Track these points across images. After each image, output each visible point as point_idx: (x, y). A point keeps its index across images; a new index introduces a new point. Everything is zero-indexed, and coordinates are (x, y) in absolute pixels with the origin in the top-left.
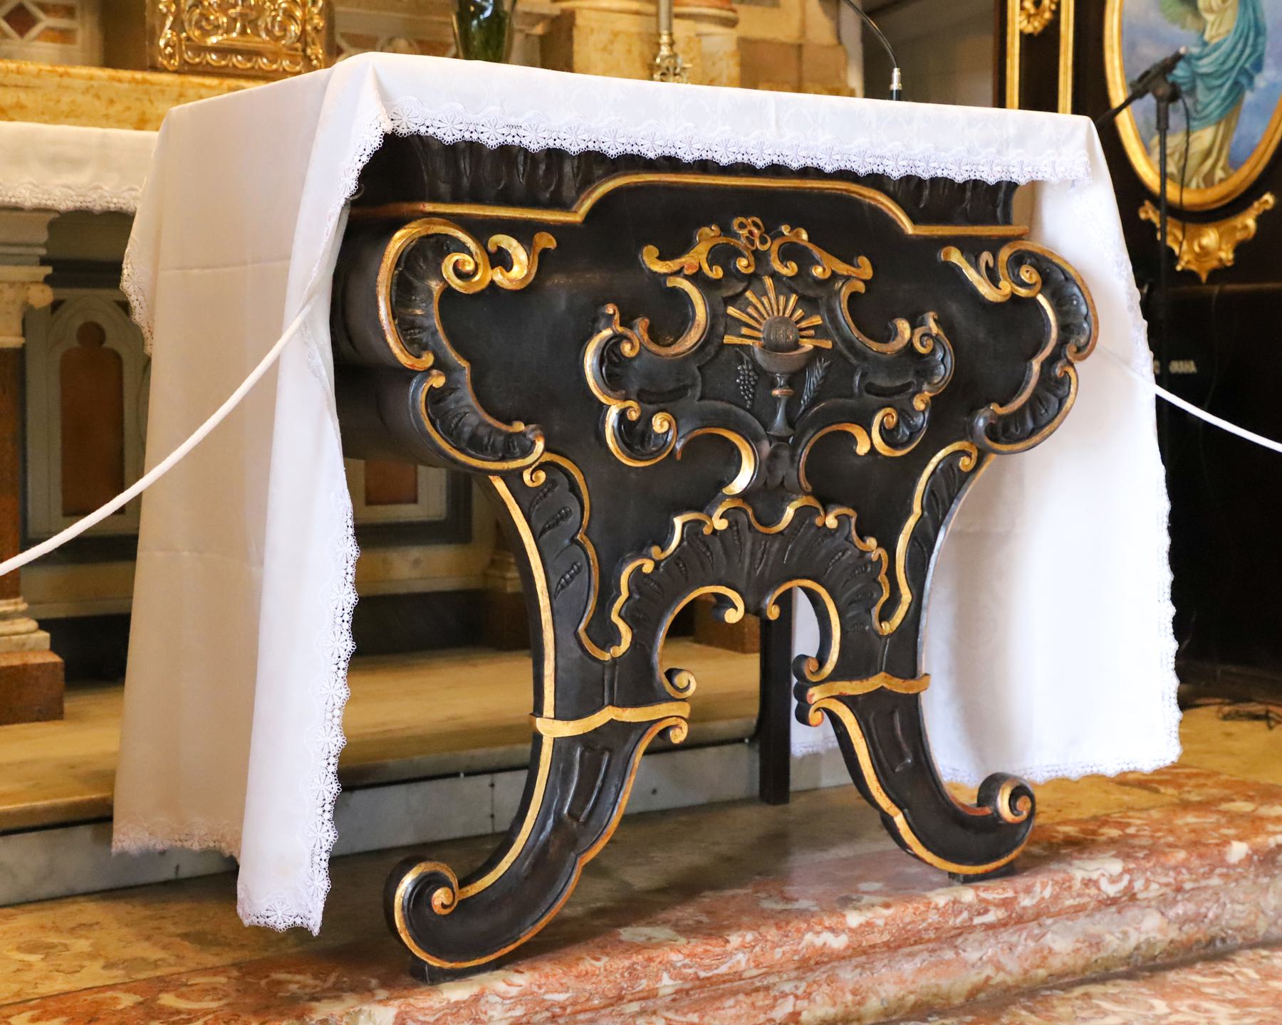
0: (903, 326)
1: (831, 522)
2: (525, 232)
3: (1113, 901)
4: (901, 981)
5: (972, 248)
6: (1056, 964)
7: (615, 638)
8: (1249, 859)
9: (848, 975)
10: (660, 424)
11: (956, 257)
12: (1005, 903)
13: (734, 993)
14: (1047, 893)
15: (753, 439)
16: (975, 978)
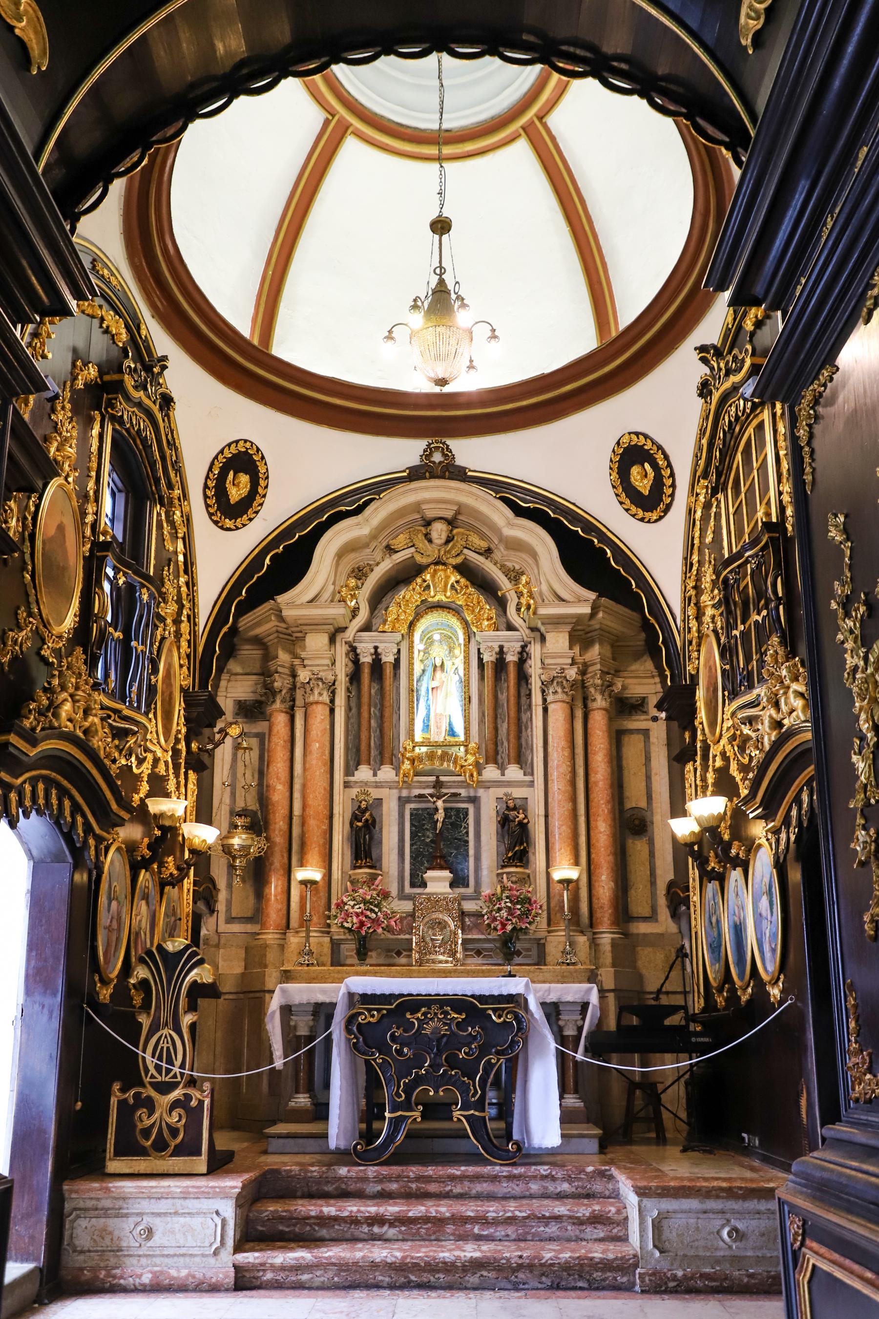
0: (470, 1029)
1: (453, 1073)
2: (378, 1010)
3: (546, 1177)
4: (482, 1187)
5: (495, 1010)
6: (532, 1191)
7: (401, 1097)
8: (594, 1172)
9: (466, 1183)
10: (405, 1050)
11: (490, 1012)
12: (508, 1171)
13: (434, 1182)
14: (523, 1170)
15: (429, 1054)
16: (505, 1190)
